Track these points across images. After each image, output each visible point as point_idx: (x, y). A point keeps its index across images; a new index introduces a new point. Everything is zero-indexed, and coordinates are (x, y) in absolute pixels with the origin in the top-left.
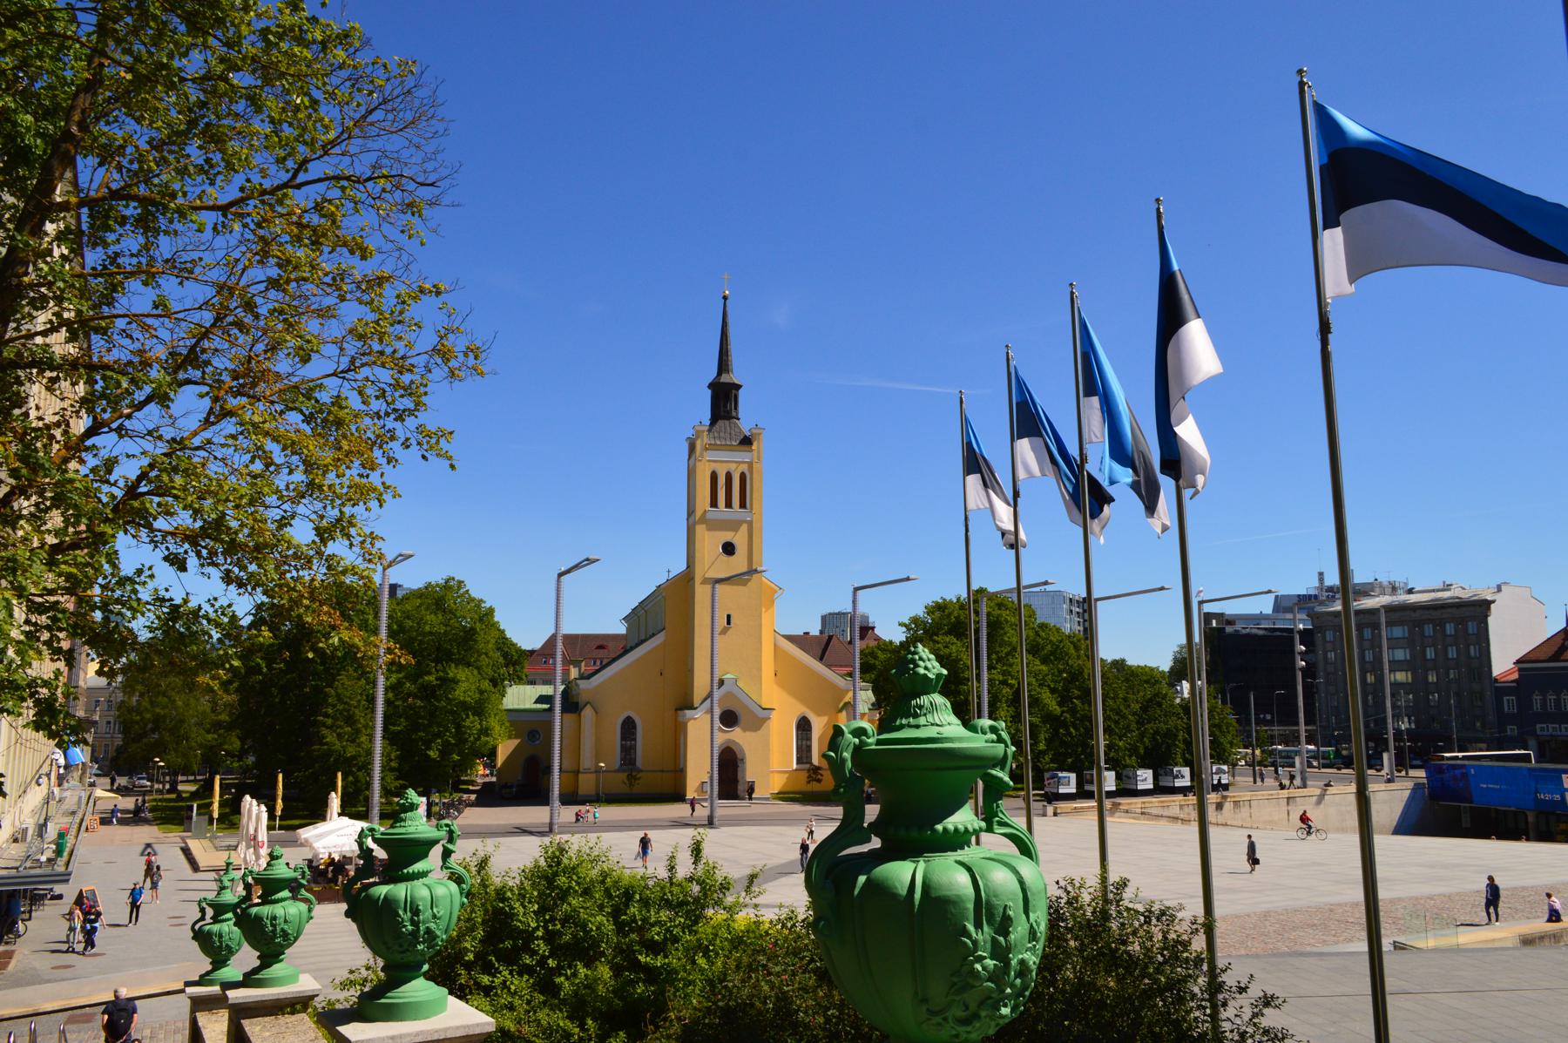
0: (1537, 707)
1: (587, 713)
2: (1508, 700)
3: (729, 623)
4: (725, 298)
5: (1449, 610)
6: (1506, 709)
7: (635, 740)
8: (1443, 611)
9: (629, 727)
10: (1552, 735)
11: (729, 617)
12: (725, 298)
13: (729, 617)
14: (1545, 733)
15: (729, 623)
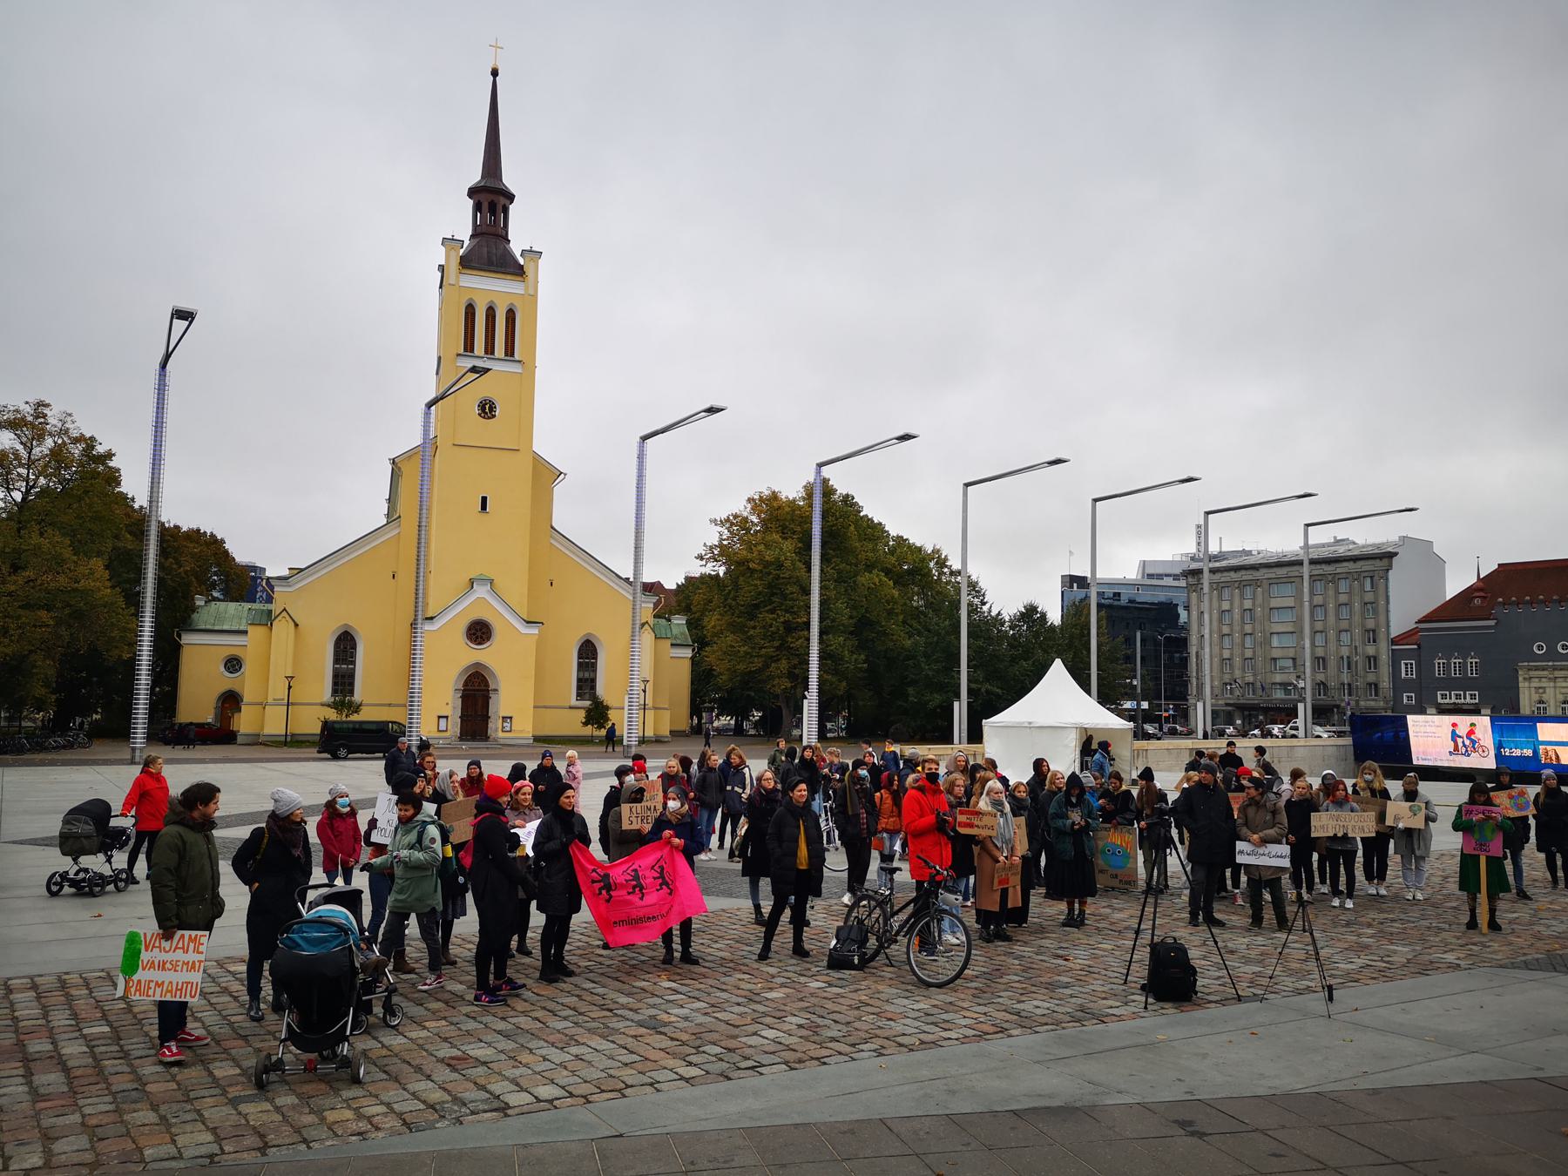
0: (1438, 673)
1: (282, 628)
2: (1406, 664)
3: (484, 507)
4: (495, 73)
5: (1345, 564)
6: (1403, 675)
7: (353, 663)
8: (1337, 565)
9: (345, 645)
10: (1454, 703)
11: (484, 500)
12: (495, 73)
13: (484, 500)
14: (1447, 701)
15: (484, 507)
